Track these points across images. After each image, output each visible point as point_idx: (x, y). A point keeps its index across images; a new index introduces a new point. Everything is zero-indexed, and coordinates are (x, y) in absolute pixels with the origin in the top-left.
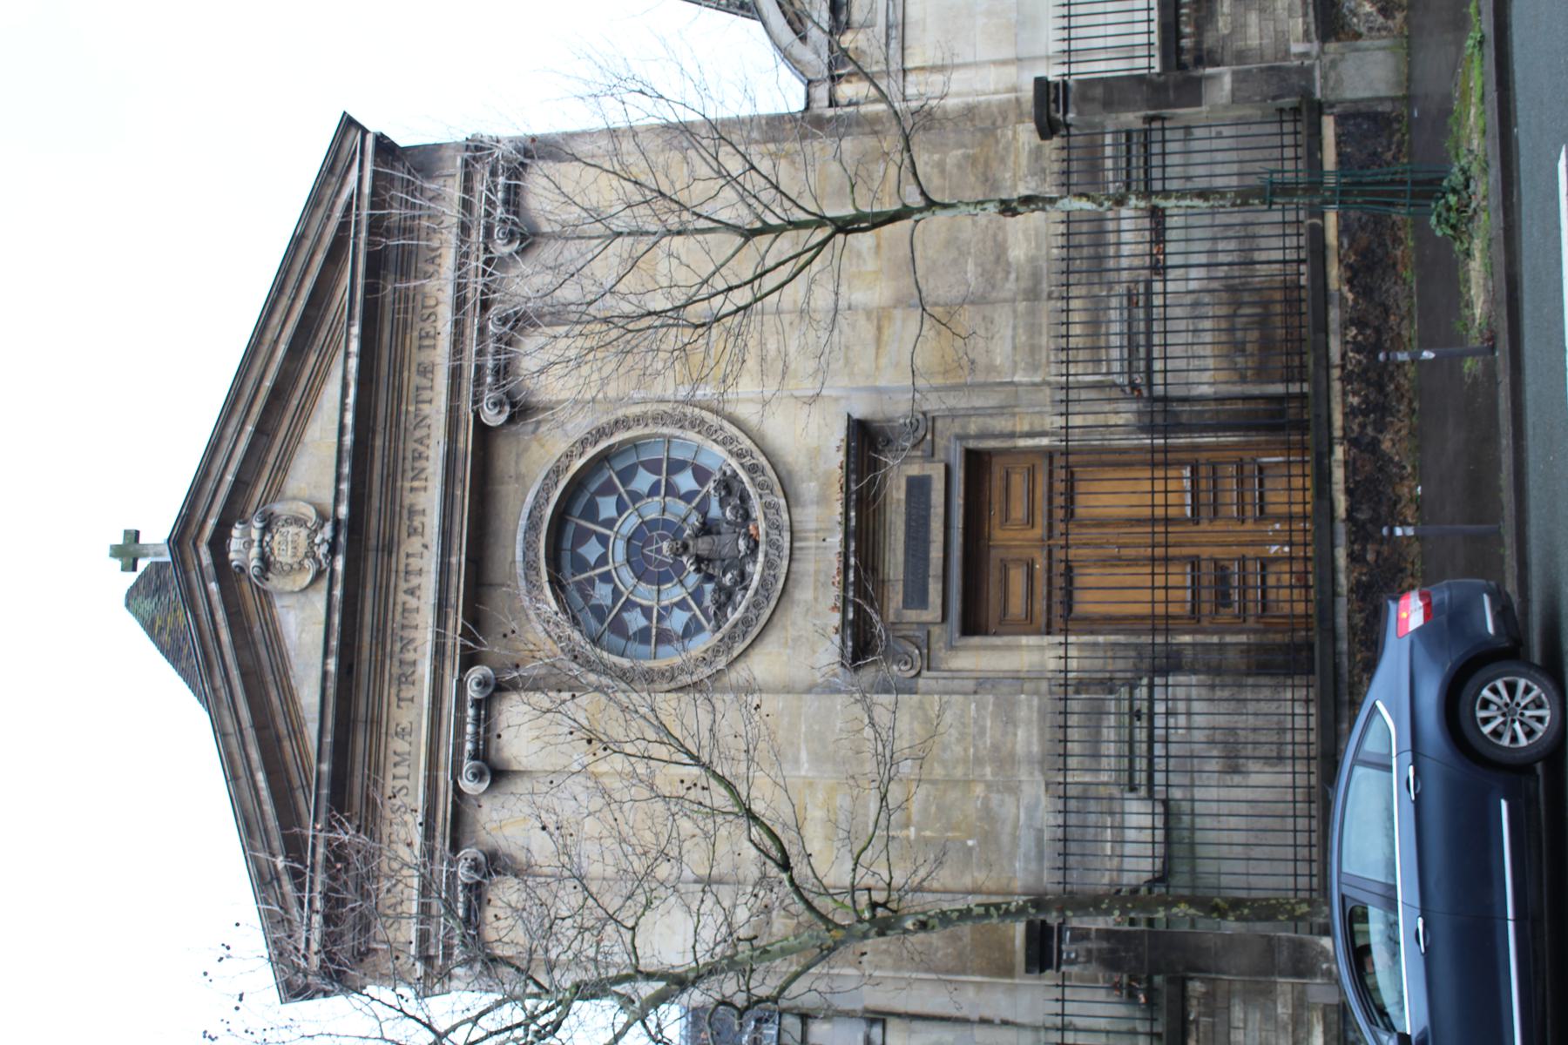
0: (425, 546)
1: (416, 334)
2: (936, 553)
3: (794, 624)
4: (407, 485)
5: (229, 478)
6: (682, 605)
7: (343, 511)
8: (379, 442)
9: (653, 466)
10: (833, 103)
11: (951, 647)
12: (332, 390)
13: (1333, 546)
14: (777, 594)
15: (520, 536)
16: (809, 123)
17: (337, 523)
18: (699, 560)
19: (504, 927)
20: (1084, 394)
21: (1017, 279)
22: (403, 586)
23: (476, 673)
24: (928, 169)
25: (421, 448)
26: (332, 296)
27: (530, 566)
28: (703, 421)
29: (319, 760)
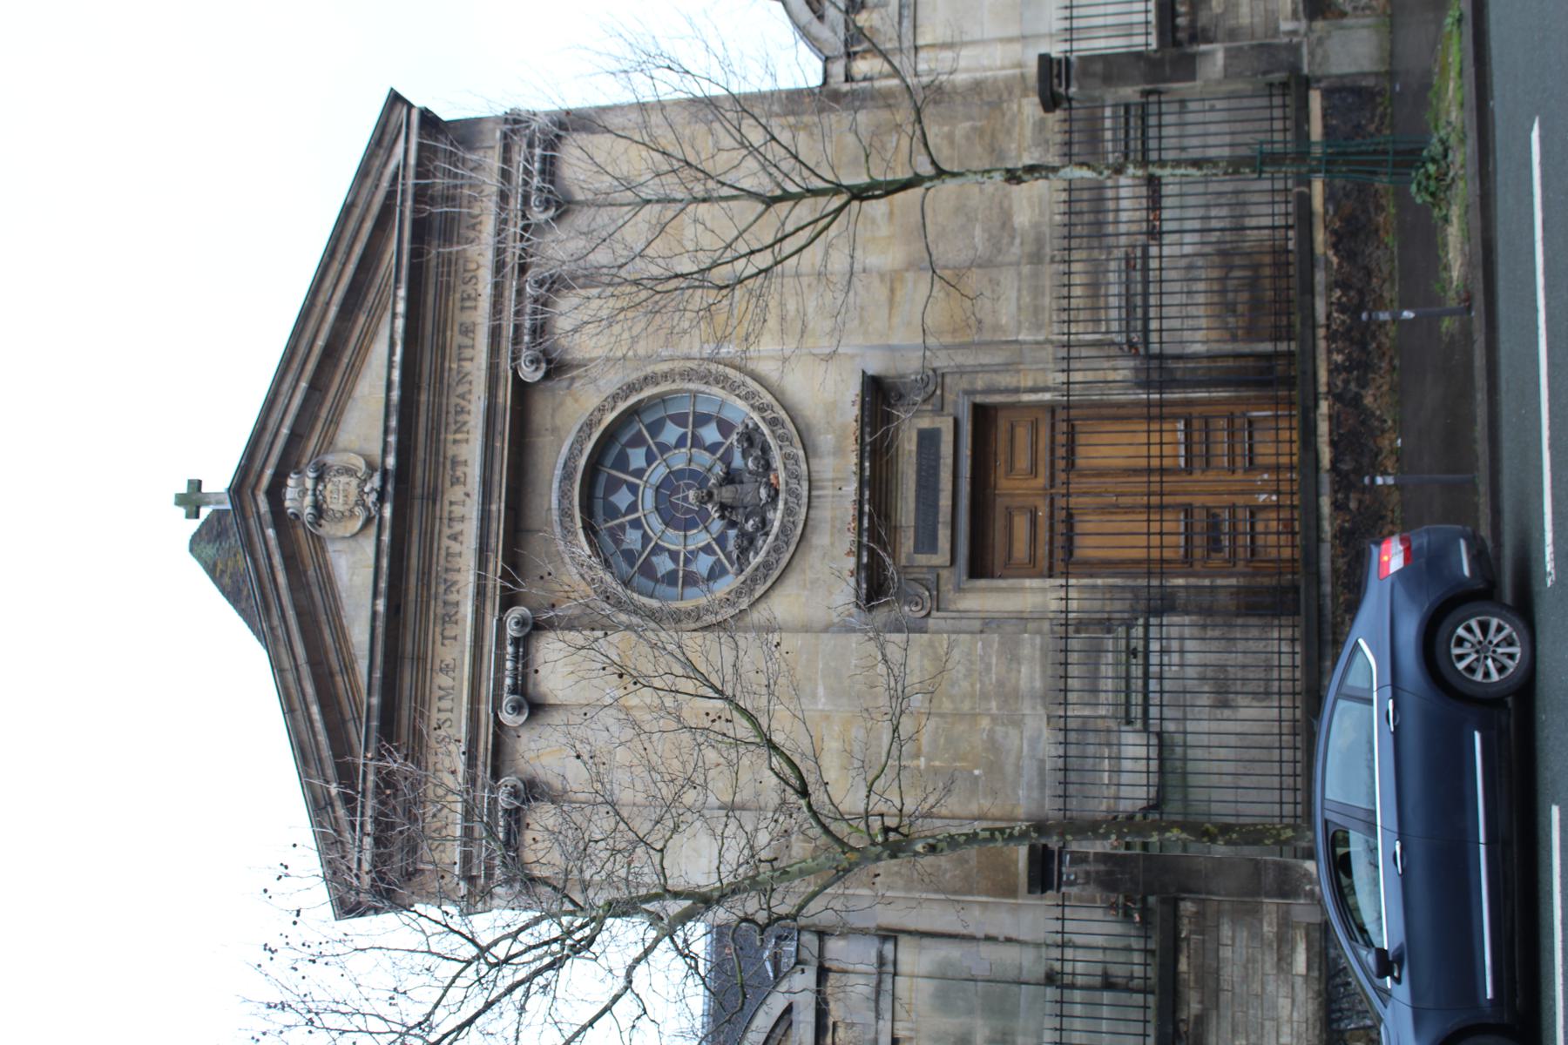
0: (467, 495)
1: (458, 296)
2: (945, 501)
3: (812, 567)
4: (450, 437)
5: (285, 431)
6: (707, 549)
7: (391, 461)
8: (423, 398)
9: (680, 420)
10: (849, 78)
11: (959, 589)
12: (380, 349)
13: (1318, 495)
14: (796, 539)
15: (555, 485)
16: (826, 97)
17: (385, 473)
18: (723, 507)
19: (542, 848)
20: (1085, 352)
21: (1022, 244)
22: (447, 531)
23: (515, 613)
24: (938, 140)
25: (463, 403)
26: (380, 260)
27: (565, 513)
28: (726, 378)
29: (369, 694)
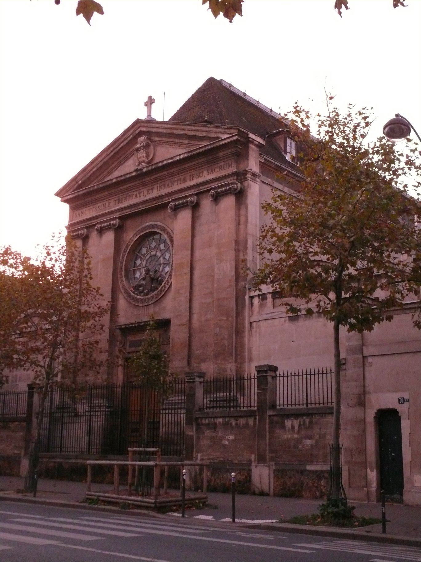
8: (165, 172)
10: (252, 298)
13: (166, 461)
27: (144, 228)
